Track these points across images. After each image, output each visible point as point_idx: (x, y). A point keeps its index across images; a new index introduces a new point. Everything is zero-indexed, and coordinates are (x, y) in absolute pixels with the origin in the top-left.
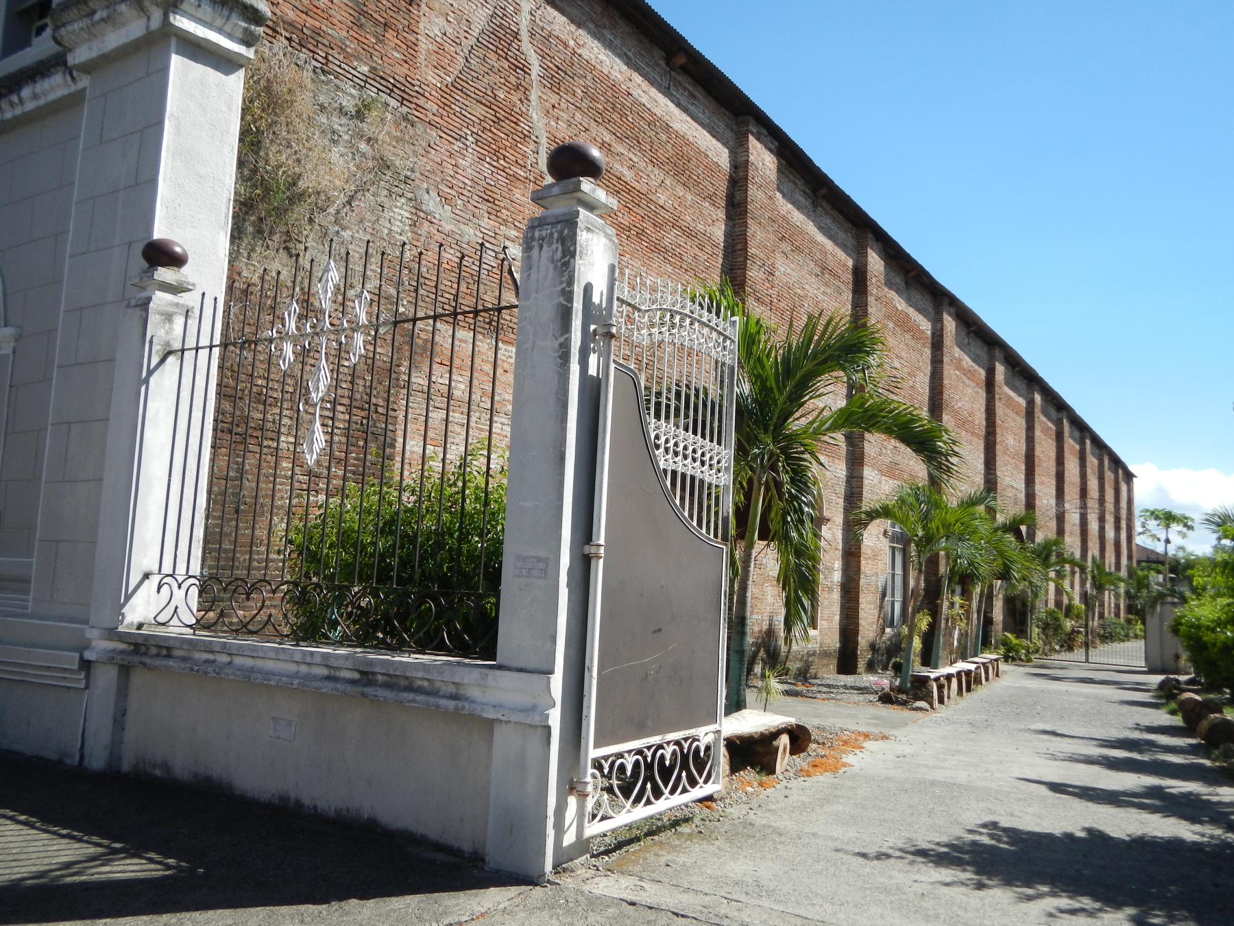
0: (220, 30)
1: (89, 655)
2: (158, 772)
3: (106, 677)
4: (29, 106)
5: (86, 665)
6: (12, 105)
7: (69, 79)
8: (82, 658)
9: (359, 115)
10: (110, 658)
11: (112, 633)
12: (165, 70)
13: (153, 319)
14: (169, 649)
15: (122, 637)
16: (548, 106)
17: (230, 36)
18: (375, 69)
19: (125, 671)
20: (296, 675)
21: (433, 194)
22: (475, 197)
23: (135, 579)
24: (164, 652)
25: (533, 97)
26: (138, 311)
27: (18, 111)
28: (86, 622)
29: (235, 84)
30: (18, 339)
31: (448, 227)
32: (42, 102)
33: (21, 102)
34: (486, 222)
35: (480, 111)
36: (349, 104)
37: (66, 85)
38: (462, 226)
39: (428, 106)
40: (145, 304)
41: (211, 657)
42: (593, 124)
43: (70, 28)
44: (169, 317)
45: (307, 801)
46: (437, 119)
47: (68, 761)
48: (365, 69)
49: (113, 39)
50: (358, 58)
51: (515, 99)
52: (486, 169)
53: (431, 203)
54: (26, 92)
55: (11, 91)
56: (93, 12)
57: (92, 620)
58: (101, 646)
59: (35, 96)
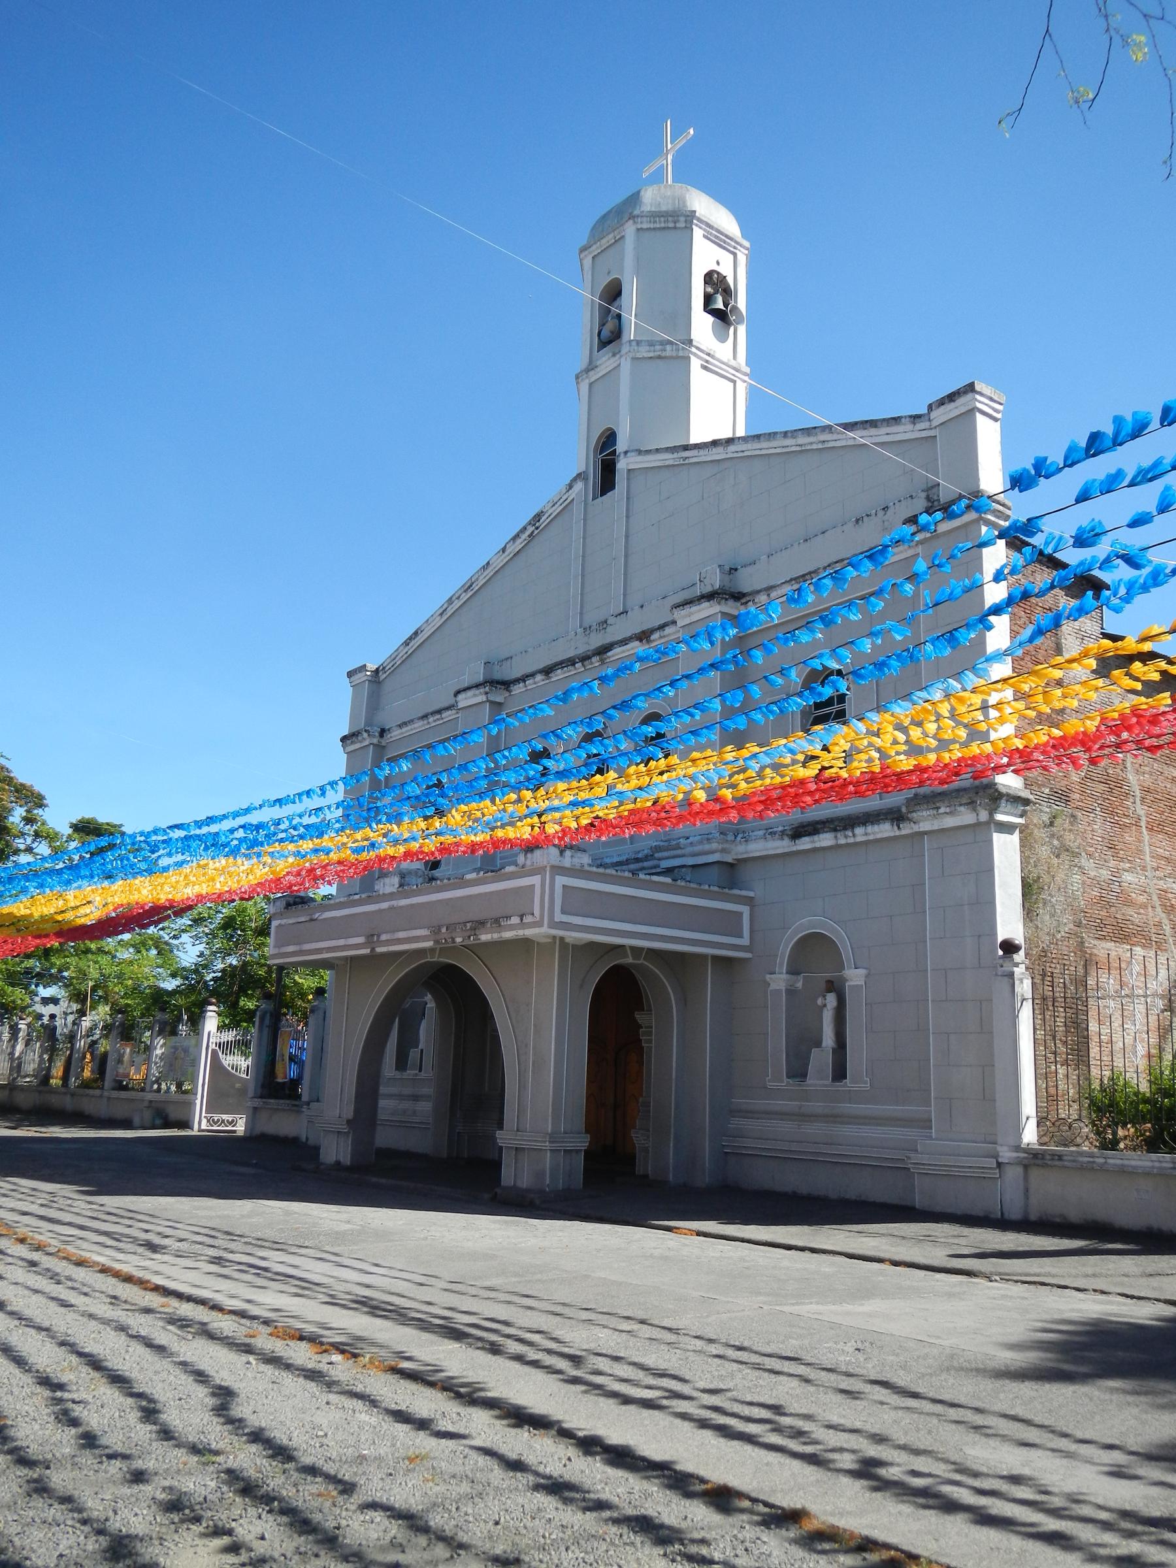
0: (1012, 814)
1: (1000, 1160)
2: (1058, 1220)
3: (1014, 1174)
4: (859, 839)
5: (999, 1165)
6: (846, 837)
7: (896, 828)
8: (997, 1162)
9: (1052, 824)
10: (1019, 1162)
11: (1018, 1148)
12: (991, 841)
13: (1017, 982)
14: (1059, 1156)
15: (1025, 1151)
16: (1137, 766)
17: (1015, 816)
18: (1051, 788)
19: (1026, 1167)
20: (1153, 1167)
21: (1083, 854)
22: (1105, 848)
23: (1024, 1120)
24: (1056, 1157)
25: (1128, 765)
26: (1006, 979)
27: (851, 840)
28: (995, 1143)
29: (1015, 837)
30: (867, 976)
31: (1092, 874)
32: (871, 837)
33: (854, 836)
34: (1112, 863)
35: (1101, 787)
36: (1046, 818)
37: (893, 830)
38: (1100, 871)
39: (1074, 797)
40: (1011, 975)
41: (1091, 1160)
42: (1165, 767)
43: (920, 814)
44: (1021, 981)
45: (1165, 1228)
46: (1080, 804)
47: (992, 1216)
48: (1047, 791)
49: (950, 822)
50: (1044, 786)
51: (1118, 771)
52: (1108, 826)
53: (1084, 861)
54: (859, 831)
55: (845, 829)
56: (938, 808)
57: (1000, 1141)
58: (1006, 1155)
59: (866, 834)
